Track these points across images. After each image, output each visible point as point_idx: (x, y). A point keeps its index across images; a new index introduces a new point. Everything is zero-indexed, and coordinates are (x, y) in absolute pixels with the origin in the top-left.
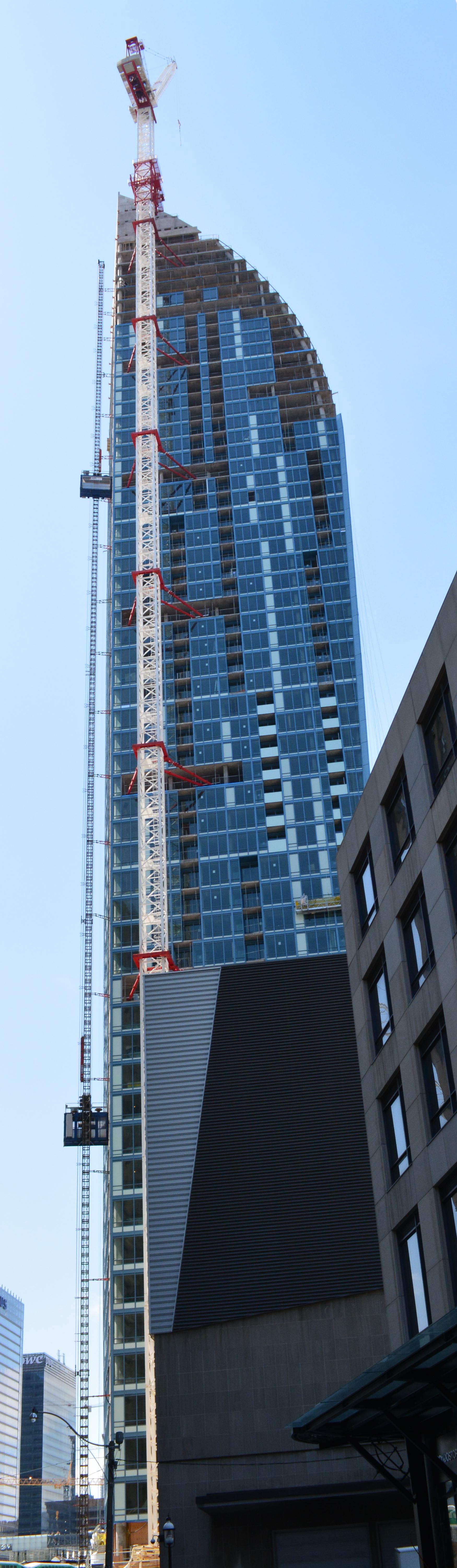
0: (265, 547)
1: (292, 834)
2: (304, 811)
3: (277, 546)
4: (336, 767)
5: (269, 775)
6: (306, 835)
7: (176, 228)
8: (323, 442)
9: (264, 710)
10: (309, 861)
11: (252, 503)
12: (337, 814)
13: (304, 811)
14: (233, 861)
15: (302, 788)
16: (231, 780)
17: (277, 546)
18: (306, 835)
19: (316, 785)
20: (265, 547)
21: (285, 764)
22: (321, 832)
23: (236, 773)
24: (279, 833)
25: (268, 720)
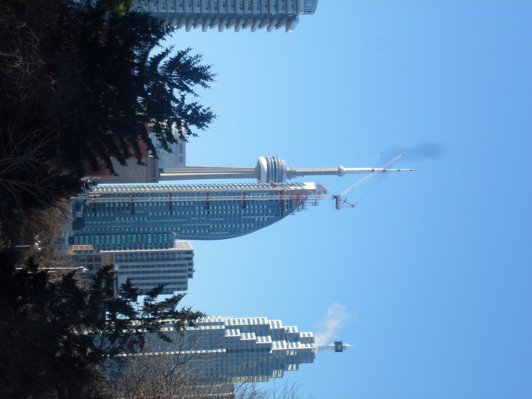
0: (184, 220)
1: (120, 222)
3: (185, 222)
5: (132, 219)
6: (119, 224)
7: (296, 204)
8: (213, 233)
9: (146, 218)
10: (115, 224)
11: (197, 218)
16: (131, 212)
17: (185, 222)
18: (119, 224)
19: (129, 226)
20: (184, 220)
21: (134, 221)
23: (133, 213)
25: (143, 219)
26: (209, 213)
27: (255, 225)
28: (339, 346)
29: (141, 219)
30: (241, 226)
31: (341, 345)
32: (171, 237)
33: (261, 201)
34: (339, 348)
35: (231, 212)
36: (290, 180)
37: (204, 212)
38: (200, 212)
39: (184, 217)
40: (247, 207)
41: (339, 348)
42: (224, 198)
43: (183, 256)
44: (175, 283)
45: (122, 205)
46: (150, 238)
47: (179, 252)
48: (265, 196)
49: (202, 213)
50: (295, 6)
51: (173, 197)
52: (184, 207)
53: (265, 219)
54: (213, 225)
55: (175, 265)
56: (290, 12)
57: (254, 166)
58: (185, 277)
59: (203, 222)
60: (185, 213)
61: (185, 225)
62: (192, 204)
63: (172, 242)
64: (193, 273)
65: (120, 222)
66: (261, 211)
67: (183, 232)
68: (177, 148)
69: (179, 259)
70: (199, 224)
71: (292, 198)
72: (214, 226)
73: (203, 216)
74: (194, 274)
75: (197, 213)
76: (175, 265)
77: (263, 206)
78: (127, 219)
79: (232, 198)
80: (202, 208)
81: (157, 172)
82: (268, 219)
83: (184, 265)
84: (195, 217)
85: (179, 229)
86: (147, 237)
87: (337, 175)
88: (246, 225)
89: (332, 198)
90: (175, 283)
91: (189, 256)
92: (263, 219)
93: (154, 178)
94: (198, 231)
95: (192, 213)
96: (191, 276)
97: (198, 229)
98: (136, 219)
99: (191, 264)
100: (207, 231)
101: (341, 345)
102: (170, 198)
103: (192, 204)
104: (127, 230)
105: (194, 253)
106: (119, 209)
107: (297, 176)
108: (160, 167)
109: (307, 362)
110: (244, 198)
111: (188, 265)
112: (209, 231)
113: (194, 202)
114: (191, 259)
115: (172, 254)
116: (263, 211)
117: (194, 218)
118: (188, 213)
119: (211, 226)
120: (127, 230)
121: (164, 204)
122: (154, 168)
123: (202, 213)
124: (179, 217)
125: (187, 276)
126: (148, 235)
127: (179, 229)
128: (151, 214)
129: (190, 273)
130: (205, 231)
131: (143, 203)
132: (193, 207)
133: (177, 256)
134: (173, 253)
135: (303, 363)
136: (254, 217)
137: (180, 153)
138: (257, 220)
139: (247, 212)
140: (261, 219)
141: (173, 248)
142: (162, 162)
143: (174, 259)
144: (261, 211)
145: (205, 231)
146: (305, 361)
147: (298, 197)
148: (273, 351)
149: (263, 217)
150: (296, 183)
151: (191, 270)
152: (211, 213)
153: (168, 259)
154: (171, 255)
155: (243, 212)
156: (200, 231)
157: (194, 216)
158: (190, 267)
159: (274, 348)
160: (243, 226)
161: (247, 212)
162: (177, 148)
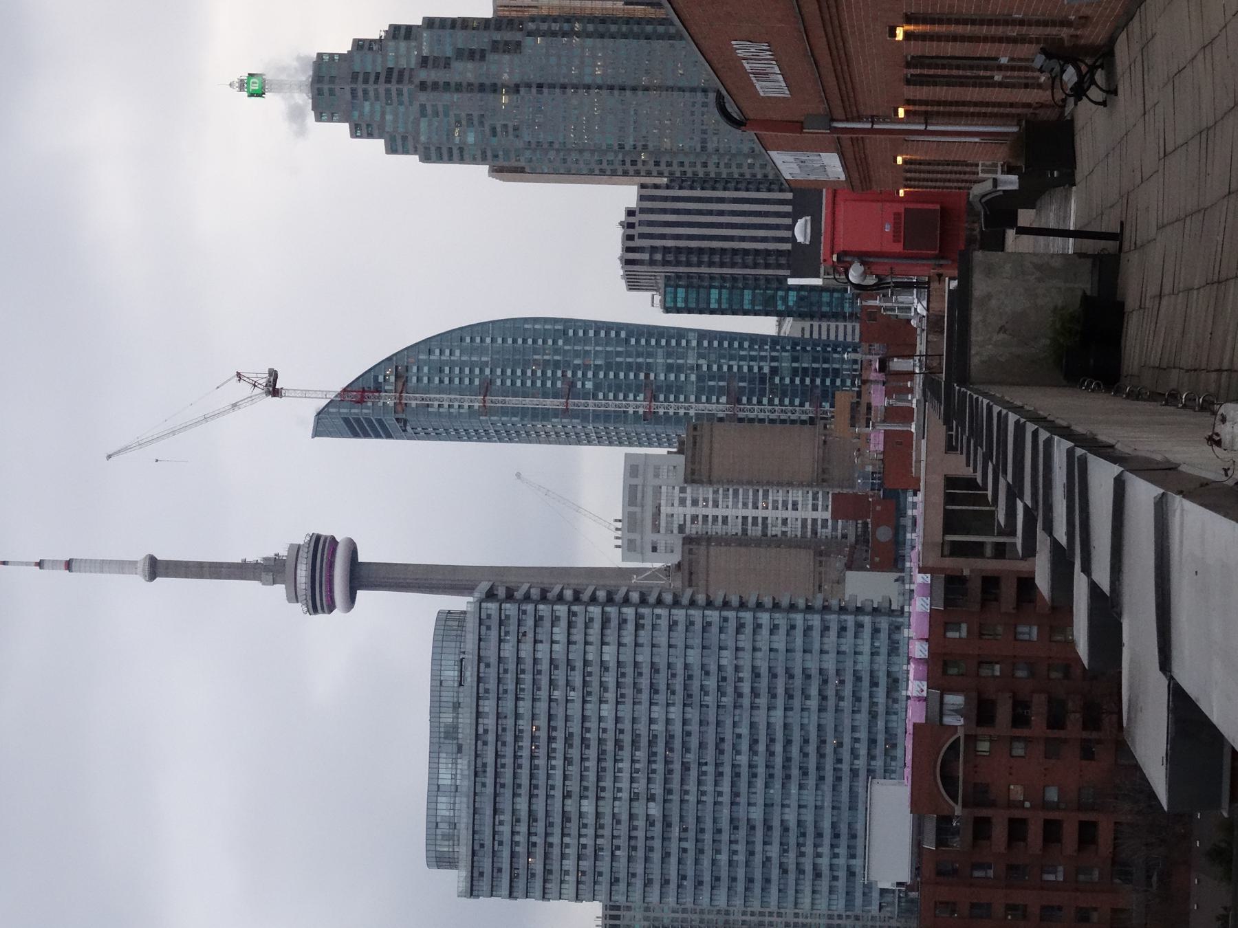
0: (618, 359)
1: (762, 364)
2: (753, 359)
3: (618, 354)
4: (736, 344)
6: (763, 358)
9: (705, 368)
10: (773, 359)
11: (592, 362)
12: (756, 347)
13: (753, 359)
14: (770, 385)
15: (742, 358)
17: (618, 354)
18: (763, 358)
19: (742, 353)
20: (618, 359)
22: (763, 354)
24: (760, 368)
25: (709, 367)
26: (564, 375)
27: (462, 340)
28: (255, 87)
29: (715, 368)
30: (493, 340)
31: (251, 88)
32: (668, 299)
33: (444, 393)
34: (256, 83)
35: (513, 372)
36: (276, 553)
37: (574, 374)
38: (584, 375)
39: (619, 364)
40: (477, 382)
41: (256, 83)
42: (529, 402)
43: (646, 256)
44: (665, 199)
45: (755, 400)
46: (713, 301)
47: (652, 262)
48: (436, 403)
49: (580, 374)
50: (484, 616)
51: (641, 411)
52: (618, 388)
53: (437, 352)
54: (556, 347)
55: (663, 237)
56: (492, 607)
57: (361, 594)
58: (642, 211)
59: (577, 354)
60: (616, 376)
61: (619, 349)
62: (601, 395)
63: (669, 289)
64: (623, 219)
65: (762, 364)
66: (447, 370)
67: (623, 334)
68: (643, 497)
69: (653, 249)
70: (587, 348)
71: (377, 394)
72: (555, 342)
73: (578, 367)
74: (622, 217)
75: (590, 375)
76: (663, 237)
77: (441, 381)
78: (745, 369)
79: (514, 402)
80: (579, 385)
81: (688, 446)
82: (430, 352)
83: (642, 236)
84: (595, 365)
85: (633, 341)
86: (719, 301)
87: (161, 556)
88: (482, 340)
89: (283, 391)
90: (665, 199)
91: (631, 256)
92: (441, 353)
93: (695, 433)
94: (591, 333)
95: (601, 375)
96: (630, 213)
97: (591, 338)
98: (725, 368)
99: (630, 238)
100: (571, 332)
101: (251, 88)
102: (650, 408)
103: (601, 395)
104: (746, 345)
105: (621, 260)
106: (762, 393)
107: (259, 561)
108: (681, 459)
109: (332, 55)
110: (485, 401)
111: (636, 237)
112: (565, 333)
113: (595, 397)
114: (628, 250)
115: (668, 261)
116: (441, 371)
117: (597, 363)
118: (612, 375)
119: (560, 342)
120: (746, 345)
121: (662, 397)
122: (693, 455)
123: (580, 374)
124: (629, 367)
125: (637, 212)
126: (716, 306)
127: (633, 341)
128: (693, 377)
129: (632, 219)
130: (575, 333)
131: (708, 401)
132: (597, 387)
133: (658, 257)
134: (665, 263)
135: (340, 55)
136: (463, 358)
137: (636, 486)
138: (457, 353)
139: (477, 371)
140: (447, 352)
141: (666, 276)
142: (674, 467)
143: (666, 250)
144: (447, 370)
145: (575, 333)
146: (336, 58)
147: (363, 397)
148: (411, 82)
149: (443, 358)
150: (356, 435)
151: (630, 226)
152: (559, 373)
153: (679, 250)
154: (672, 259)
155: (487, 371)
156: (585, 333)
157: (598, 368)
158: (631, 232)
159: (406, 89)
160: (488, 340)
161: (477, 371)
162: (643, 497)
